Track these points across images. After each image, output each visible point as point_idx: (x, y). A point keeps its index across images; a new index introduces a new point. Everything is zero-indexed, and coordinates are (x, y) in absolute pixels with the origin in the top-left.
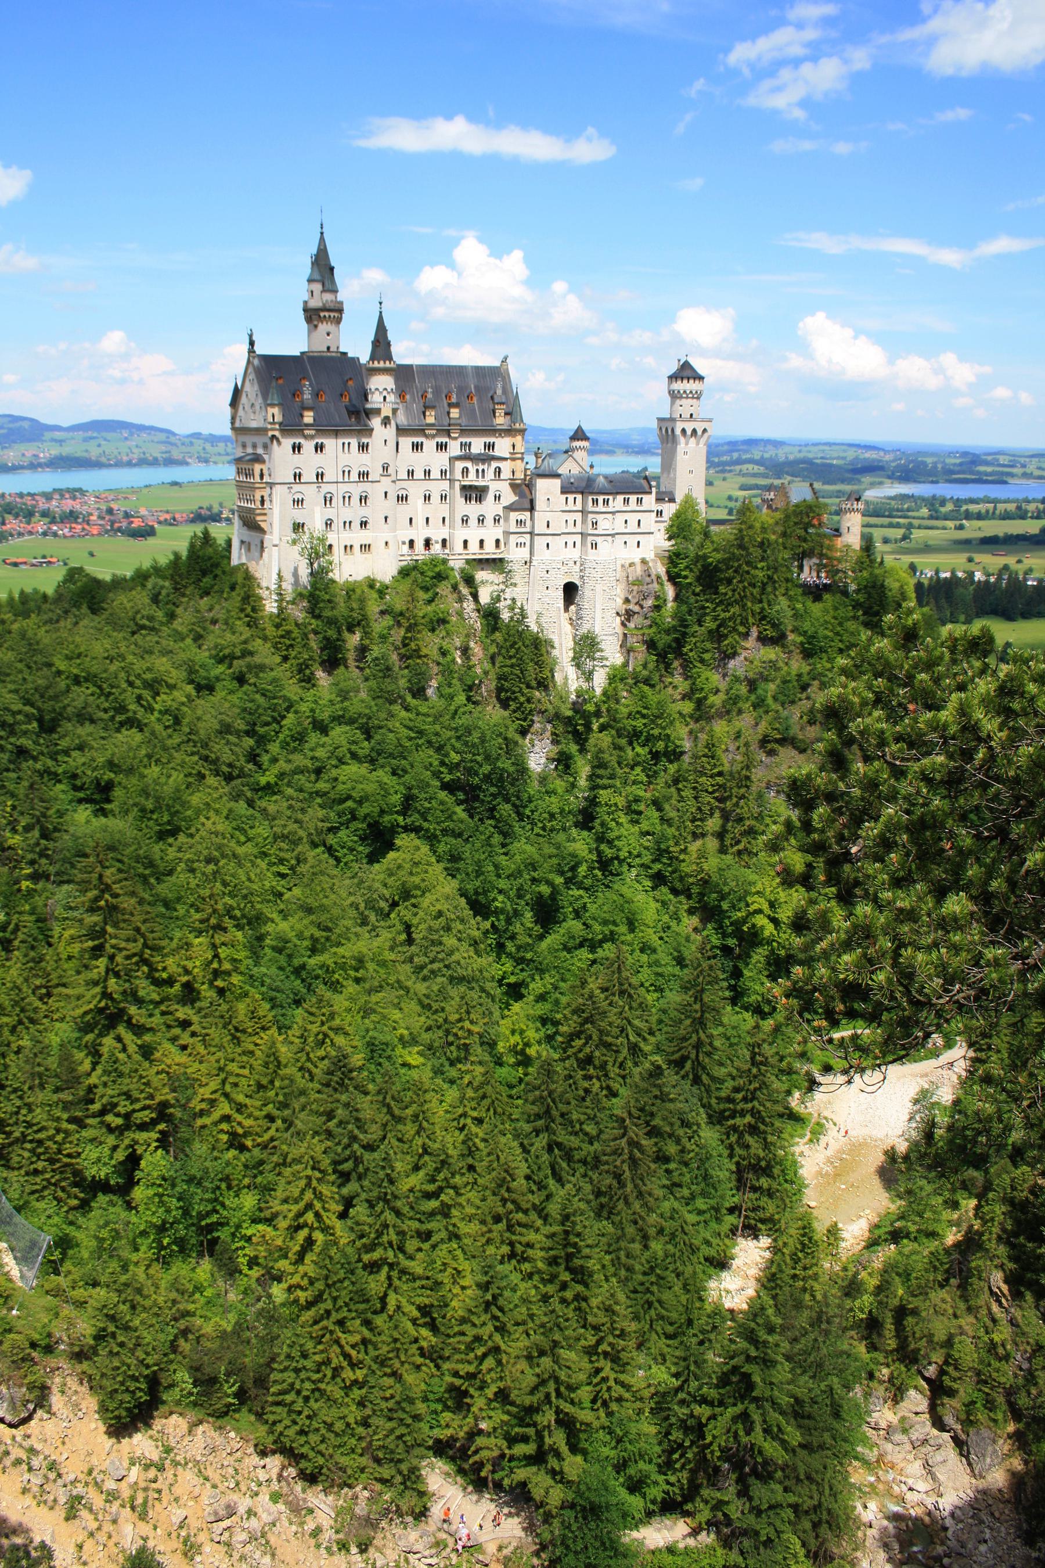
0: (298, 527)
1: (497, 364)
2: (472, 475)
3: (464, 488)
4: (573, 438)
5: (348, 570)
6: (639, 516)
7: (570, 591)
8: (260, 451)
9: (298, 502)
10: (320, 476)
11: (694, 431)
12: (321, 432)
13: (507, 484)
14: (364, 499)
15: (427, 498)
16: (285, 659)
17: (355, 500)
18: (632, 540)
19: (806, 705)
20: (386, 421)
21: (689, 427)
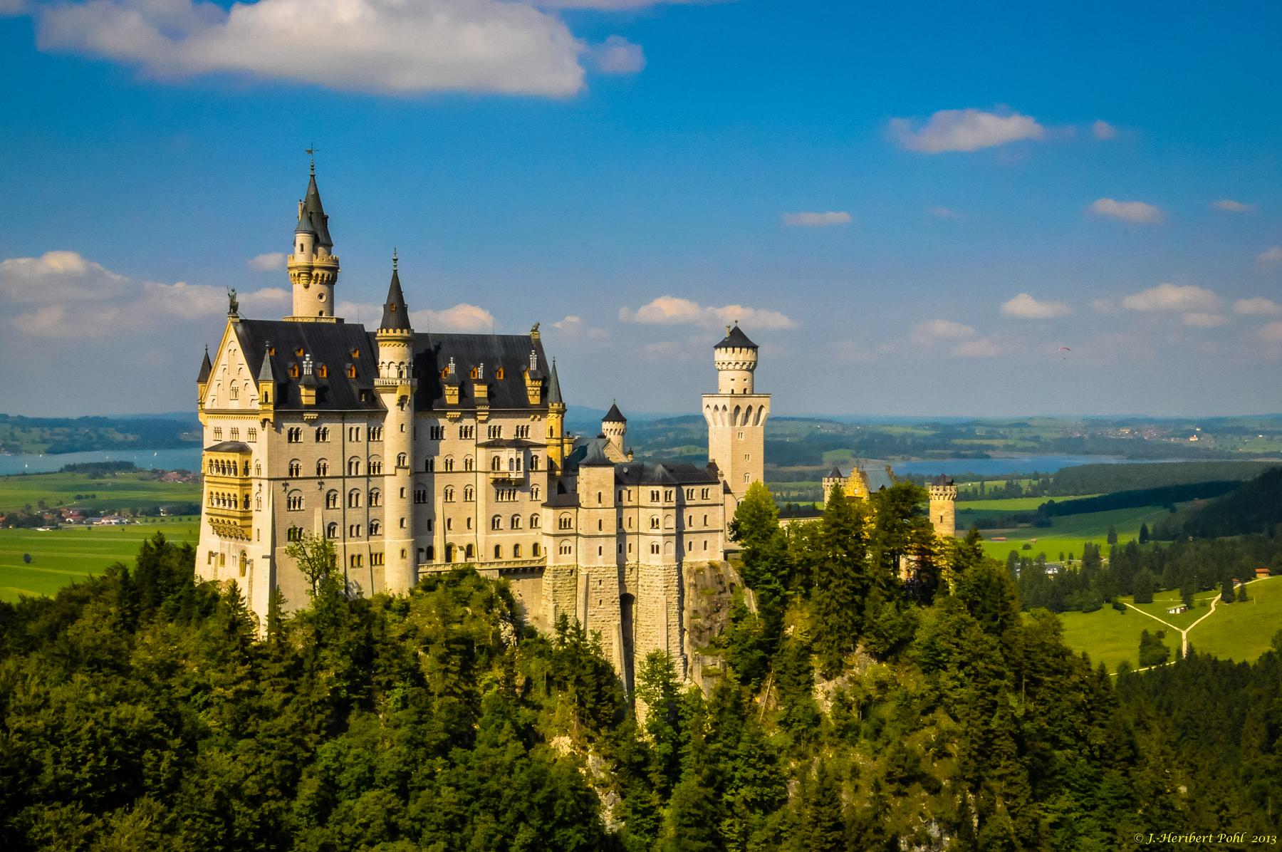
0: (295, 534)
1: (528, 333)
2: (504, 467)
3: (496, 482)
4: (605, 420)
5: (363, 583)
6: (705, 510)
7: (626, 601)
8: (243, 438)
9: (293, 503)
10: (321, 469)
11: (750, 408)
12: (324, 416)
13: (545, 475)
14: (373, 497)
15: (448, 495)
16: (286, 702)
17: (362, 501)
18: (698, 540)
19: (932, 734)
20: (401, 403)
21: (744, 404)
